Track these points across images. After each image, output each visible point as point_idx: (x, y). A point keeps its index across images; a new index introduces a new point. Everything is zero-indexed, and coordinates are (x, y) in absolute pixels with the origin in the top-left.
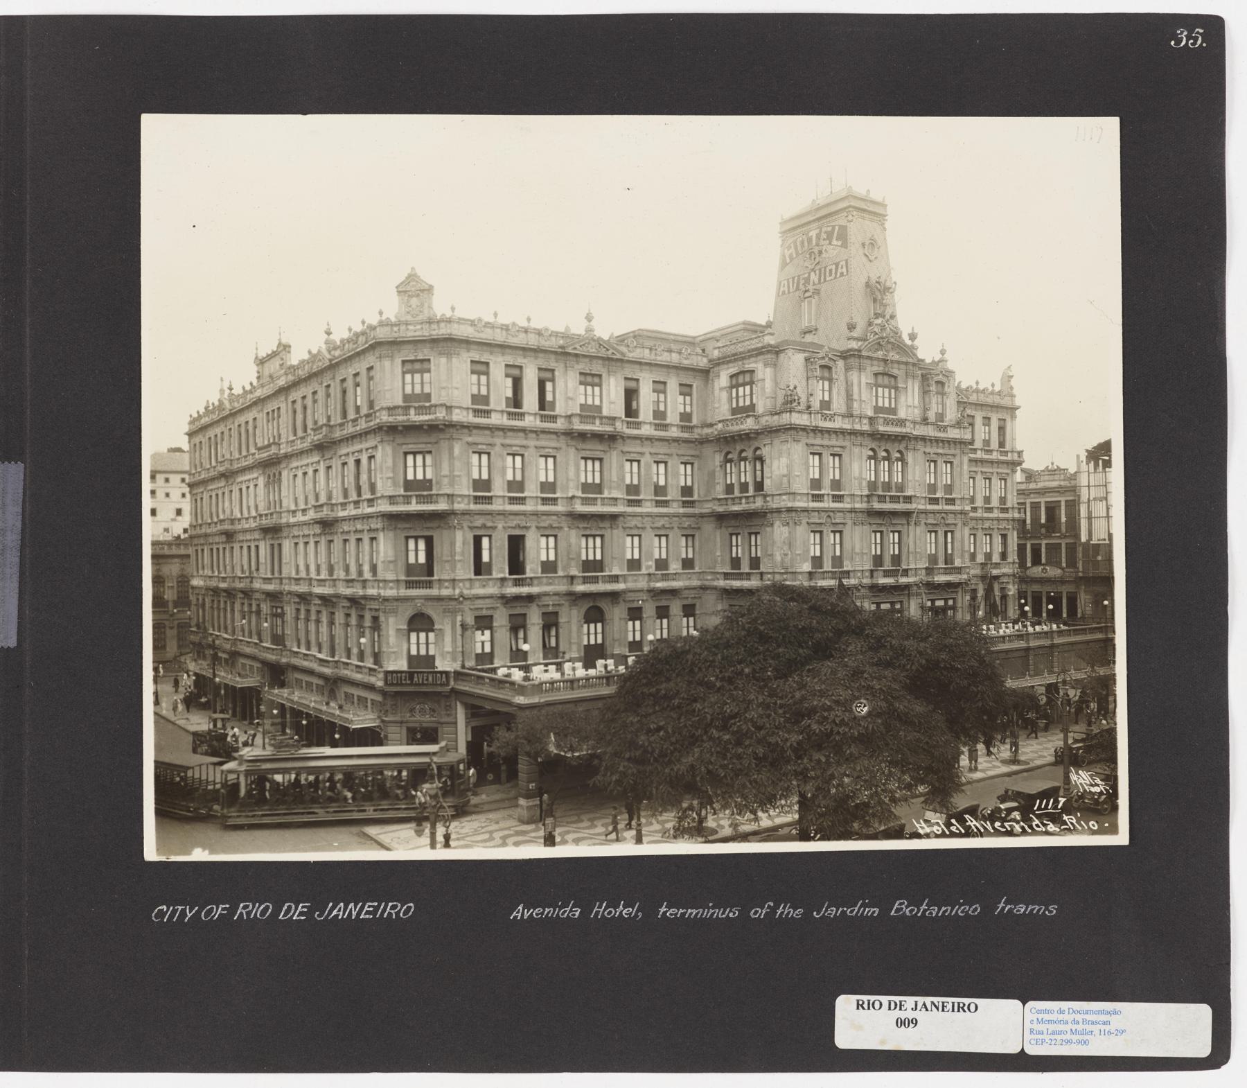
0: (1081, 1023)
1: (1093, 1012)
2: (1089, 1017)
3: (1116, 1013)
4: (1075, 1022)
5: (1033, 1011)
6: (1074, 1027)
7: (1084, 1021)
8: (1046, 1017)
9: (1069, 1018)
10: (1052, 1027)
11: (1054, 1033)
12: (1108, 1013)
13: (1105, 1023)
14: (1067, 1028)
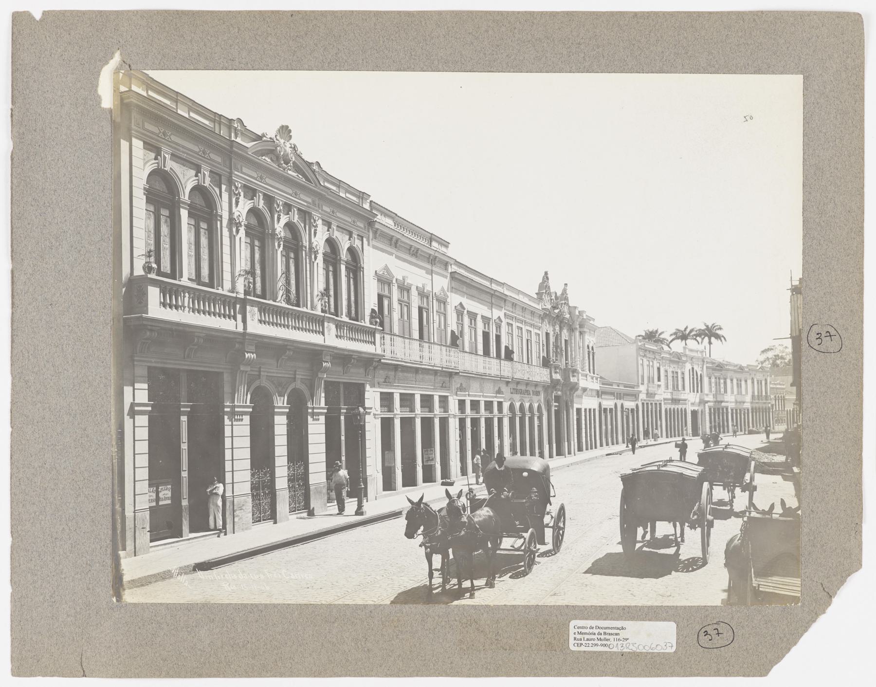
0: (603, 634)
1: (611, 628)
2: (608, 631)
3: (623, 628)
4: (600, 634)
5: (576, 627)
6: (599, 637)
7: (605, 633)
8: (583, 631)
9: (596, 631)
10: (586, 637)
11: (588, 640)
12: (618, 629)
13: (616, 634)
14: (595, 637)
